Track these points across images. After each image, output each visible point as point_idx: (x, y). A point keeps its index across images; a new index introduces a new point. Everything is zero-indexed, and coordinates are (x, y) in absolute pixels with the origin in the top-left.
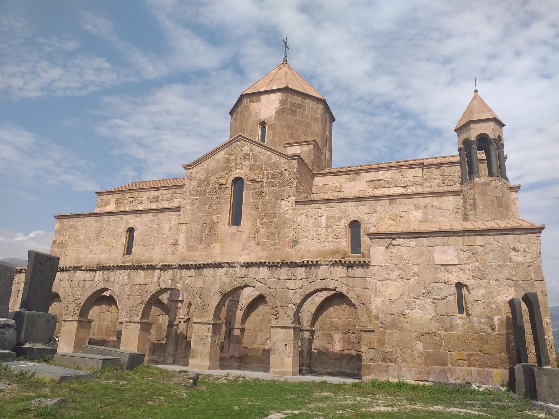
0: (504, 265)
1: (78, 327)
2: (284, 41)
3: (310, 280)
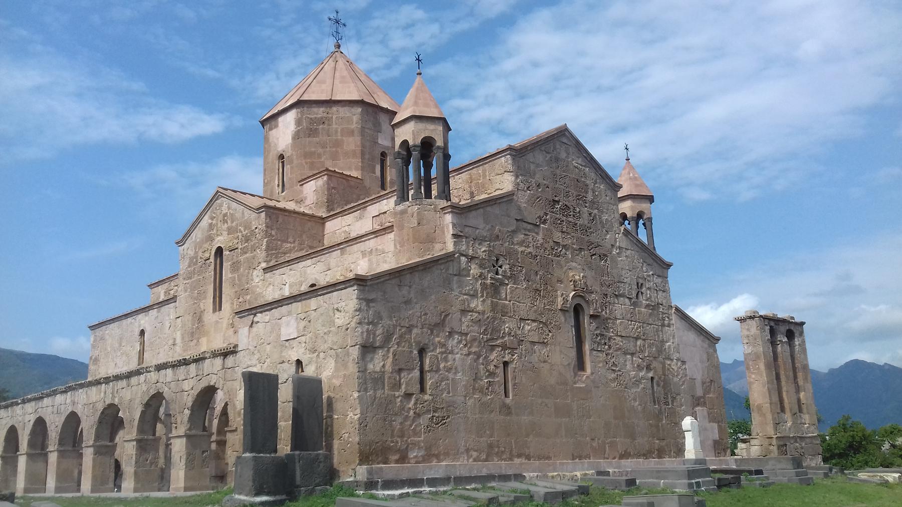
0: (329, 332)
1: (58, 458)
2: (330, 19)
3: (199, 378)
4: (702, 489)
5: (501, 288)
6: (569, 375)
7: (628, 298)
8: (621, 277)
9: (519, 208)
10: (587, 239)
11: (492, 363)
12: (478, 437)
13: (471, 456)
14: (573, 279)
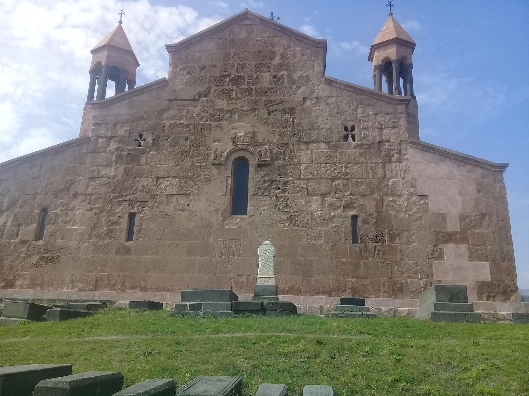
4: (202, 313)
5: (143, 155)
6: (215, 220)
7: (325, 142)
8: (316, 125)
9: (174, 91)
10: (264, 99)
11: (117, 214)
12: (87, 272)
13: (77, 286)
14: (233, 136)
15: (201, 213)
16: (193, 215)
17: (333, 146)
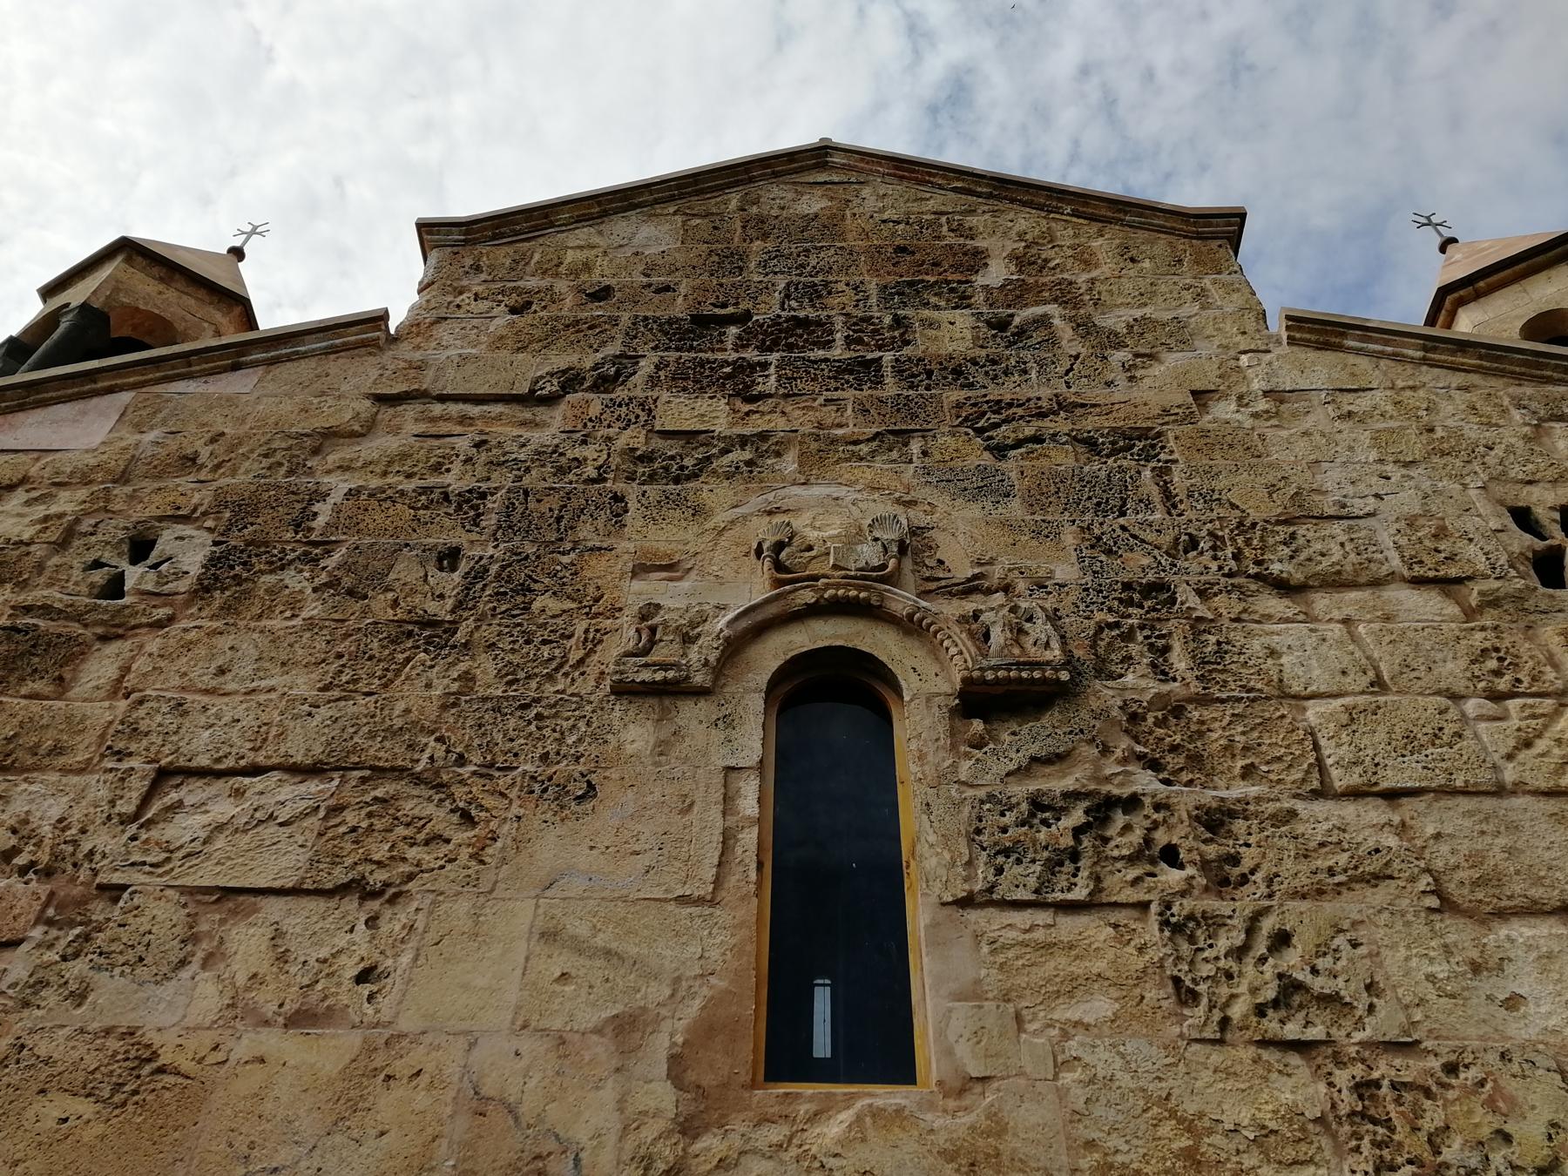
7: (1418, 582)
15: (472, 1045)
16: (401, 1067)
17: (1492, 601)
